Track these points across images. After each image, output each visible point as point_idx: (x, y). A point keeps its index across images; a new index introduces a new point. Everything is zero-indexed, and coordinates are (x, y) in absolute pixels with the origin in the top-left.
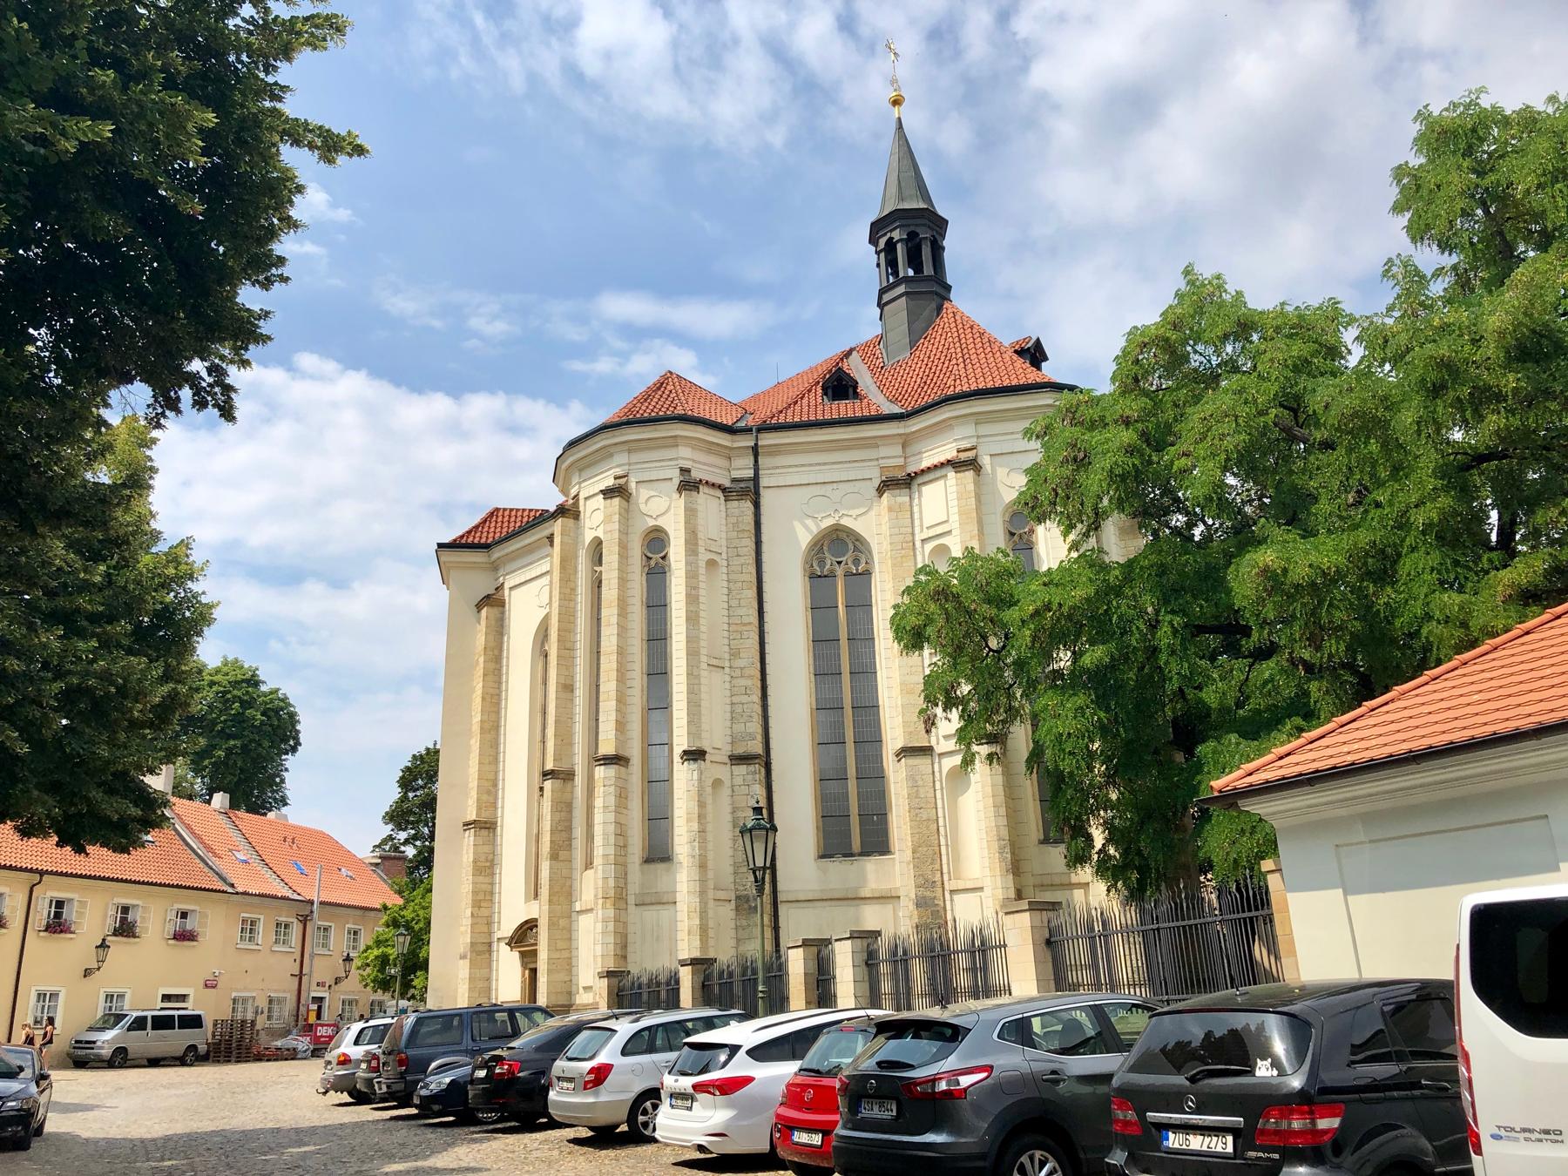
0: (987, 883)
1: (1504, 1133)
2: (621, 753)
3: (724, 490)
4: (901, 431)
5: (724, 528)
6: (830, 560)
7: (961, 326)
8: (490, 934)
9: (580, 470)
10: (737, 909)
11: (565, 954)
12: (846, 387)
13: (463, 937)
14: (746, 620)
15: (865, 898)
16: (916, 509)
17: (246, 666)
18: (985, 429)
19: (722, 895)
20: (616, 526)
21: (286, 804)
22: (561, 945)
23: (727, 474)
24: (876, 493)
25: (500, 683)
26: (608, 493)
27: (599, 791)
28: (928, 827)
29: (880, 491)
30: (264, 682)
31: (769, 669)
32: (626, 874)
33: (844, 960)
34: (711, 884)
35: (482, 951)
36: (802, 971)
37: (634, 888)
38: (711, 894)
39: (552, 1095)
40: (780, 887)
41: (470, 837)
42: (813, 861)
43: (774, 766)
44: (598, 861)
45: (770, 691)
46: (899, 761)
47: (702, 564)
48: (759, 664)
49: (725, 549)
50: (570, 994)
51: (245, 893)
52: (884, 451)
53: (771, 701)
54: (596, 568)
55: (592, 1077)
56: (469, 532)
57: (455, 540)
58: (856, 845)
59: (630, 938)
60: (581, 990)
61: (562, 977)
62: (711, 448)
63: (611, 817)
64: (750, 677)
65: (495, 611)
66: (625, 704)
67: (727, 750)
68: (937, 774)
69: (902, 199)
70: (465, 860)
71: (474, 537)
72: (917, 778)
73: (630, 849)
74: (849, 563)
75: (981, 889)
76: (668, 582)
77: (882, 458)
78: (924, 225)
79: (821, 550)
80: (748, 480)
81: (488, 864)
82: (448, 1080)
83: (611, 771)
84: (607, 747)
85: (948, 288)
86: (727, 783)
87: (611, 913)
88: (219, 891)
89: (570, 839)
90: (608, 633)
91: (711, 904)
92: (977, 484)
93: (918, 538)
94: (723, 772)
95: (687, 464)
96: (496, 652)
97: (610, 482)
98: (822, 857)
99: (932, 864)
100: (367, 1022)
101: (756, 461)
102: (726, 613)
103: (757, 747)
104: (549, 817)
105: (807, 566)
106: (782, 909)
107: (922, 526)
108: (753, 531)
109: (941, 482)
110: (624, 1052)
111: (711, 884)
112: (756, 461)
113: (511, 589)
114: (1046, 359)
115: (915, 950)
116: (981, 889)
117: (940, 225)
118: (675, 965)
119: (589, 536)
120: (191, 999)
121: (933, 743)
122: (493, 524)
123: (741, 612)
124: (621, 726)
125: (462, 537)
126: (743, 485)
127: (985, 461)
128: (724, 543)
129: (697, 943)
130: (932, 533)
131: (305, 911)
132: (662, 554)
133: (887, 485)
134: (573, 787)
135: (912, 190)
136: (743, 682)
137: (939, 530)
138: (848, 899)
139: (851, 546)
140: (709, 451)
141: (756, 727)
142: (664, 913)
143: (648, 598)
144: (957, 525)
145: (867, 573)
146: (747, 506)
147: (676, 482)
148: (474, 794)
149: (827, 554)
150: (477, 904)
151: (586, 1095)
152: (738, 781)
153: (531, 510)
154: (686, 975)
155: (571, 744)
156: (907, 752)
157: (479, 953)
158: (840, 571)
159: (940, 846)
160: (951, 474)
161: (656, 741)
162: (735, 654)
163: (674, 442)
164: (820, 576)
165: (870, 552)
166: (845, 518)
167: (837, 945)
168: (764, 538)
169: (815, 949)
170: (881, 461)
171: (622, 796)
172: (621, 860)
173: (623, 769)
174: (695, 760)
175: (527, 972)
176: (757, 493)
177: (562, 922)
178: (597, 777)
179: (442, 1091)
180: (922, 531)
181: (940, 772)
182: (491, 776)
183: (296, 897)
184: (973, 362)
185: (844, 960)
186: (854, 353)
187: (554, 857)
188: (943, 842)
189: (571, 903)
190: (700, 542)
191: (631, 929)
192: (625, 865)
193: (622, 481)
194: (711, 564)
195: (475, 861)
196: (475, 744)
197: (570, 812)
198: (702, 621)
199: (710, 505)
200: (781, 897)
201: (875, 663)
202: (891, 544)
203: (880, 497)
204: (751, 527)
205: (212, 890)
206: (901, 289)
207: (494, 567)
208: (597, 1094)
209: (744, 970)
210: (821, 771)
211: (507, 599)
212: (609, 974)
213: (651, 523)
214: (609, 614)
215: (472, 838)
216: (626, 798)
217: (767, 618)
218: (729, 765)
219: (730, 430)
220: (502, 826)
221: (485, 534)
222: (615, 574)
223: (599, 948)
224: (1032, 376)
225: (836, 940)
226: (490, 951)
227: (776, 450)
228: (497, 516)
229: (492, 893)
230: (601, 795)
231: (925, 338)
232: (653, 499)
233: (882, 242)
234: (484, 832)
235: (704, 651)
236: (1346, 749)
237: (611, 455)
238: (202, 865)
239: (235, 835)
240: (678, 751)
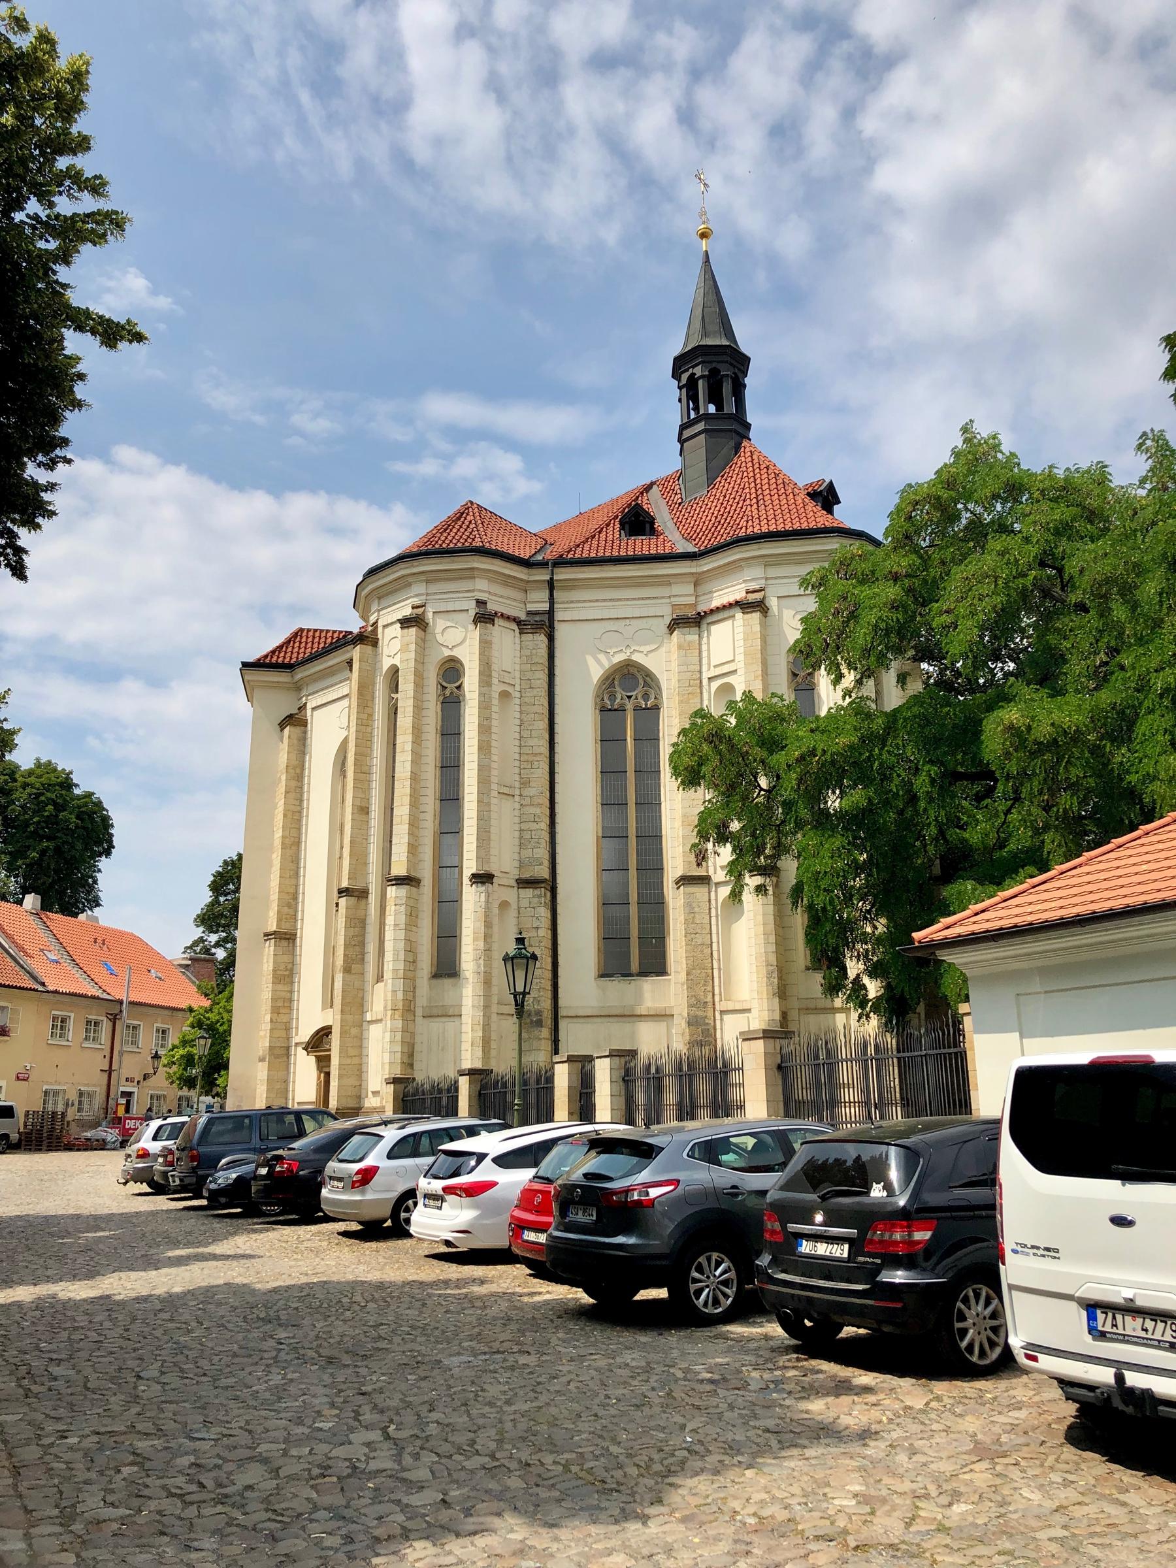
0: (755, 1005)
1: (1021, 1248)
2: (413, 874)
3: (519, 622)
4: (693, 570)
5: (518, 660)
6: (620, 693)
7: (757, 465)
8: (288, 1038)
9: (380, 598)
11: (356, 1061)
12: (644, 523)
13: (263, 1041)
14: (536, 750)
15: (641, 1016)
16: (704, 647)
17: (59, 769)
18: (773, 572)
20: (413, 655)
21: (98, 905)
22: (352, 1052)
23: (522, 606)
24: (666, 630)
25: (301, 801)
26: (405, 623)
27: (391, 909)
28: (702, 951)
30: (77, 785)
31: (558, 798)
32: (414, 988)
33: (603, 1074)
34: (495, 999)
35: (280, 1054)
36: (566, 1084)
37: (422, 1001)
38: (495, 1008)
39: (325, 1192)
40: (561, 1003)
41: (269, 948)
44: (388, 975)
45: (558, 819)
46: (678, 888)
47: (495, 695)
49: (518, 681)
50: (359, 1098)
51: (56, 992)
52: (676, 589)
54: (393, 695)
55: (359, 1177)
56: (273, 652)
57: (259, 660)
58: (635, 966)
59: (417, 1048)
60: (370, 1094)
61: (352, 1081)
62: (507, 581)
63: (402, 934)
64: (539, 805)
65: (297, 730)
66: (418, 828)
67: (515, 874)
68: (713, 902)
69: (705, 334)
70: (265, 966)
71: (278, 657)
72: (694, 905)
73: (420, 965)
74: (639, 697)
75: (748, 1011)
76: (462, 712)
77: (674, 596)
78: (727, 362)
79: (612, 685)
80: (543, 613)
81: (287, 973)
82: (234, 1176)
84: (399, 868)
85: (748, 426)
86: (514, 906)
87: (399, 1024)
88: (31, 989)
89: (363, 954)
90: (402, 759)
91: (494, 1017)
92: (763, 625)
93: (705, 676)
94: (511, 895)
95: (483, 596)
96: (298, 771)
97: (407, 611)
98: (602, 976)
99: (704, 985)
100: (165, 1119)
101: (552, 595)
102: (517, 743)
104: (343, 933)
105: (598, 700)
106: (562, 1024)
107: (709, 664)
108: (547, 664)
109: (730, 622)
110: (390, 1156)
111: (495, 999)
112: (552, 595)
113: (314, 709)
114: (838, 502)
115: (667, 1069)
116: (748, 1011)
117: (741, 362)
118: (452, 1074)
119: (386, 663)
121: (711, 872)
122: (297, 645)
123: (531, 742)
124: (413, 849)
125: (266, 656)
126: (537, 618)
127: (773, 603)
128: (517, 674)
129: (480, 1053)
130: (719, 671)
131: (114, 1011)
132: (457, 684)
133: (678, 623)
134: (367, 904)
135: (715, 326)
136: (532, 810)
137: (725, 669)
138: (624, 1016)
139: (641, 682)
141: (543, 853)
142: (450, 1025)
143: (442, 726)
144: (742, 664)
145: (656, 708)
146: (541, 640)
147: (472, 613)
148: (274, 907)
149: (618, 689)
150: (275, 1010)
151: (355, 1193)
152: (525, 903)
153: (334, 632)
154: (464, 1083)
155: (366, 864)
156: (685, 880)
157: (277, 1057)
158: (629, 706)
159: (712, 969)
160: (739, 615)
161: (446, 865)
162: (525, 783)
163: (471, 574)
164: (610, 710)
165: (659, 688)
166: (636, 654)
167: (597, 1062)
168: (557, 671)
169: (579, 1065)
170: (672, 599)
171: (412, 915)
172: (410, 974)
173: (414, 889)
174: (483, 883)
175: (322, 1075)
176: (552, 627)
177: (354, 1031)
178: (388, 896)
179: (229, 1185)
180: (709, 669)
181: (716, 900)
182: (292, 890)
183: (105, 996)
184: (767, 504)
185: (603, 1074)
186: (655, 487)
187: (347, 970)
188: (716, 965)
189: (363, 1013)
190: (494, 674)
191: (418, 1039)
192: (414, 980)
193: (420, 611)
194: (505, 695)
195: (274, 970)
196: (276, 858)
197: (364, 927)
198: (494, 751)
199: (505, 638)
200: (562, 1013)
201: (660, 794)
202: (679, 681)
205: (23, 988)
206: (701, 426)
207: (298, 688)
208: (363, 1193)
210: (604, 896)
211: (309, 718)
212: (395, 1081)
213: (447, 653)
214: (404, 740)
215: (272, 948)
216: (417, 917)
217: (557, 749)
218: (516, 888)
219: (527, 563)
220: (301, 938)
221: (289, 654)
222: (410, 702)
223: (387, 1057)
224: (822, 519)
225: (597, 1058)
226: (288, 1055)
227: (572, 585)
228: (301, 637)
229: (291, 1000)
230: (392, 913)
231: (723, 476)
232: (448, 630)
233: (685, 377)
234: (284, 943)
235: (494, 780)
236: (1030, 909)
237: (409, 585)
238: (13, 964)
239: (47, 938)
240: (467, 874)
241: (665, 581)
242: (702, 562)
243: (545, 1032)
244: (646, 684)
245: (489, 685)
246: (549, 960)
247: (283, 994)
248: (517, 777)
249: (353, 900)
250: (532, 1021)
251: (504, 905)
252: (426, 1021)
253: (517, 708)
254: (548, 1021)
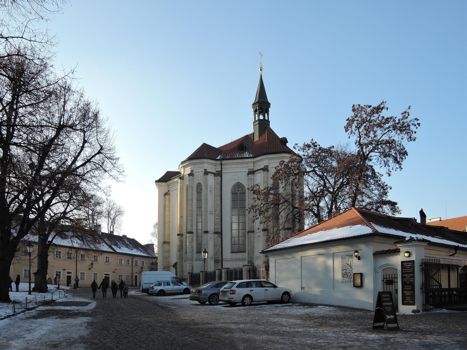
5: (214, 183)
14: (218, 204)
16: (255, 179)
18: (271, 161)
26: (189, 175)
42: (230, 254)
43: (223, 234)
45: (223, 219)
48: (220, 213)
53: (223, 221)
64: (218, 216)
67: (213, 231)
72: (251, 238)
83: (190, 235)
94: (212, 235)
98: (232, 252)
101: (221, 167)
103: (219, 230)
112: (221, 167)
114: (288, 142)
117: (269, 105)
120: (110, 275)
121: (255, 230)
123: (217, 202)
126: (218, 173)
127: (269, 169)
128: (214, 186)
140: (211, 165)
141: (219, 227)
146: (219, 178)
152: (215, 237)
156: (249, 232)
157: (167, 268)
158: (239, 193)
162: (215, 211)
168: (223, 185)
171: (192, 240)
177: (181, 263)
194: (211, 191)
197: (183, 242)
199: (211, 178)
204: (220, 183)
209: (210, 273)
235: (208, 211)
241: (247, 163)
242: (255, 159)
243: (220, 264)
245: (207, 189)
246: (221, 249)
247: (168, 255)
248: (214, 210)
249: (180, 237)
251: (211, 237)
252: (196, 261)
253: (214, 194)
254: (221, 262)
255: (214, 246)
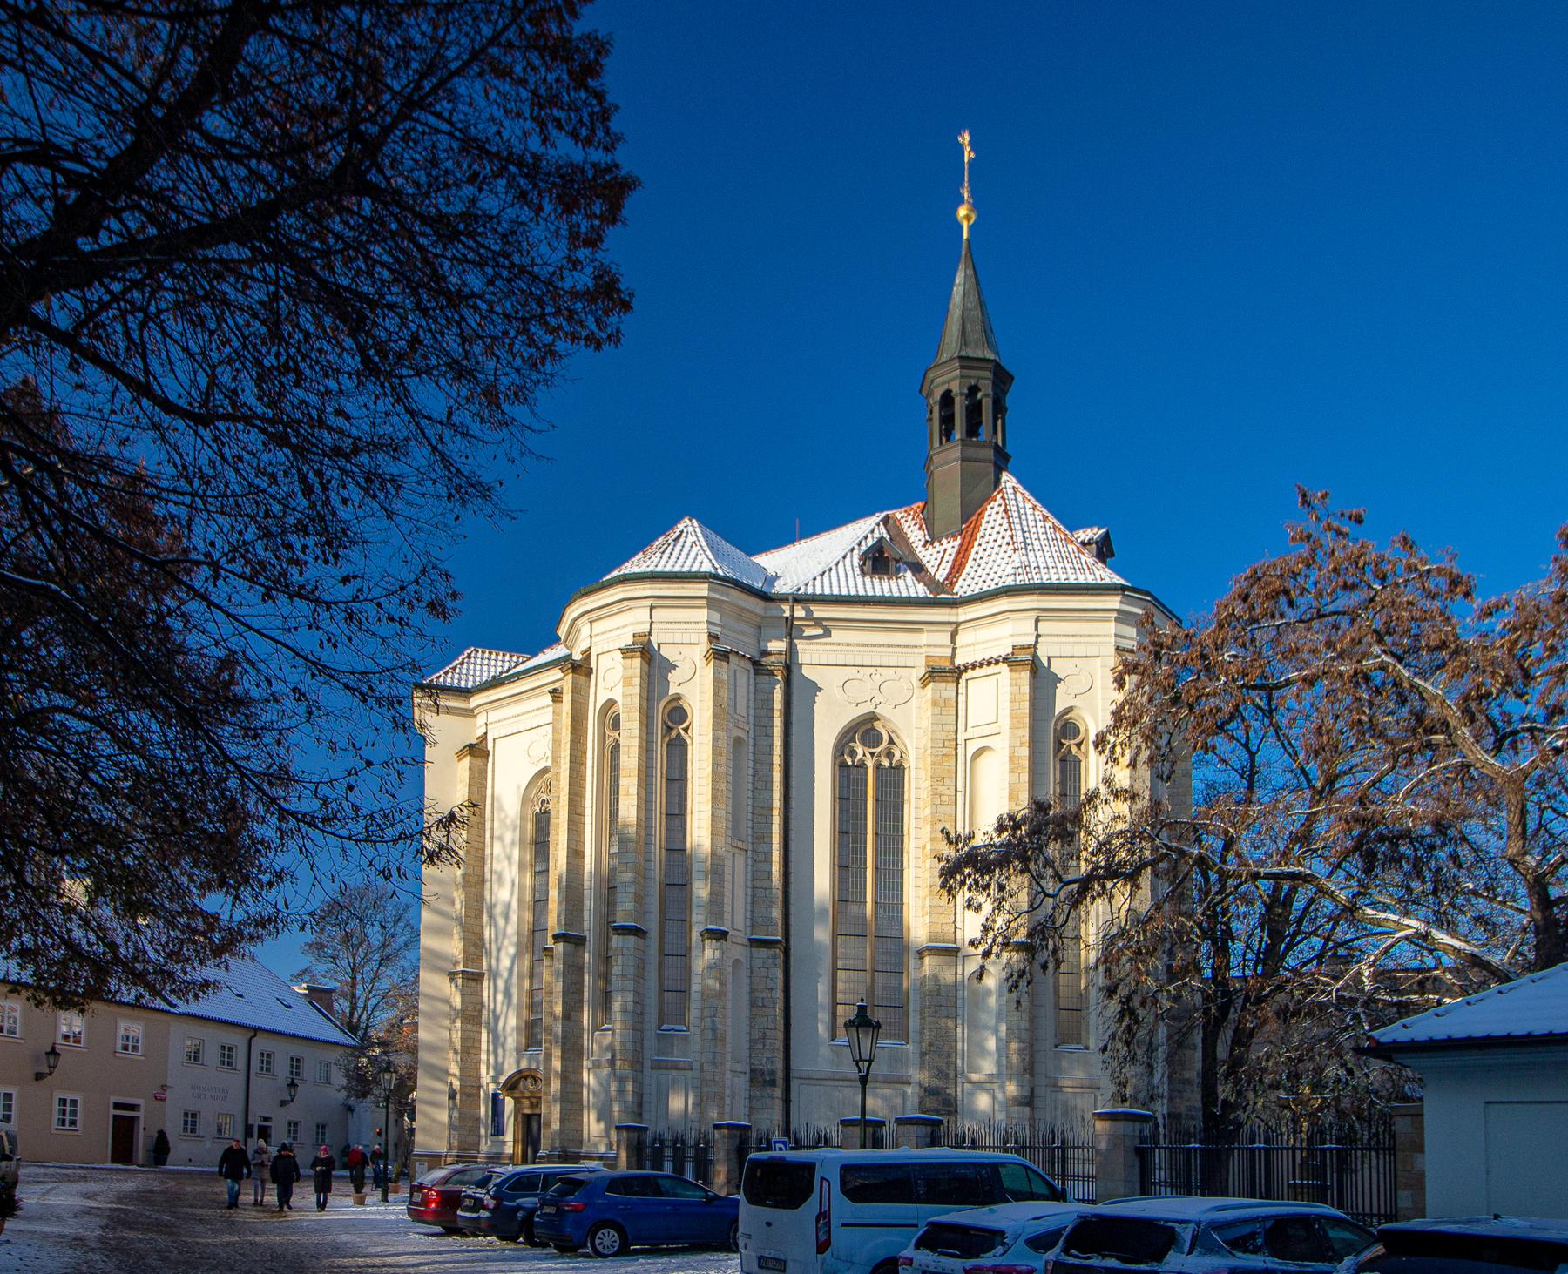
10: (751, 1081)
19: (738, 1067)
29: (924, 682)
31: (793, 856)
40: (795, 1065)
43: (792, 952)
59: (646, 1098)
132: (685, 725)
133: (934, 674)
145: (899, 769)
152: (758, 963)
171: (641, 967)
192: (641, 1031)
203: (923, 687)
243: (778, 1092)
244: (891, 741)
246: (782, 1021)
250: (765, 1081)
254: (780, 1082)
255: (753, 1004)
